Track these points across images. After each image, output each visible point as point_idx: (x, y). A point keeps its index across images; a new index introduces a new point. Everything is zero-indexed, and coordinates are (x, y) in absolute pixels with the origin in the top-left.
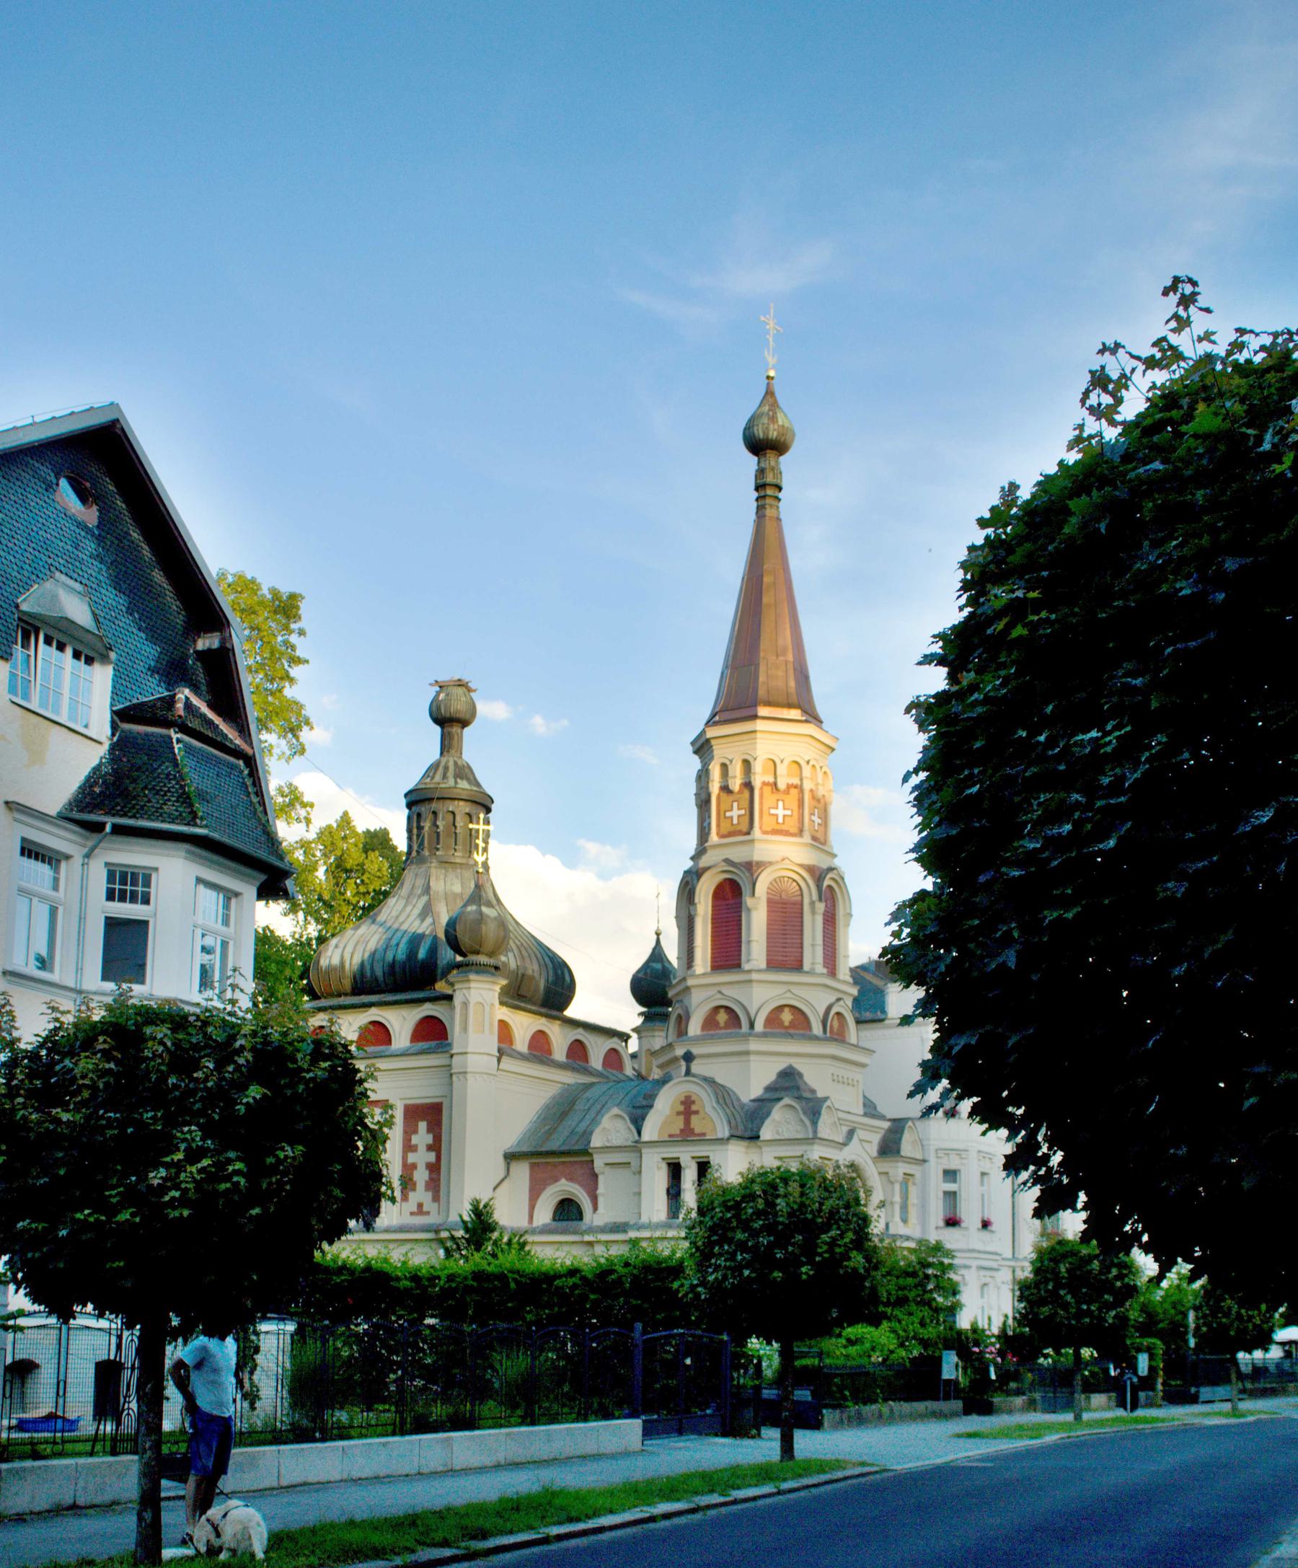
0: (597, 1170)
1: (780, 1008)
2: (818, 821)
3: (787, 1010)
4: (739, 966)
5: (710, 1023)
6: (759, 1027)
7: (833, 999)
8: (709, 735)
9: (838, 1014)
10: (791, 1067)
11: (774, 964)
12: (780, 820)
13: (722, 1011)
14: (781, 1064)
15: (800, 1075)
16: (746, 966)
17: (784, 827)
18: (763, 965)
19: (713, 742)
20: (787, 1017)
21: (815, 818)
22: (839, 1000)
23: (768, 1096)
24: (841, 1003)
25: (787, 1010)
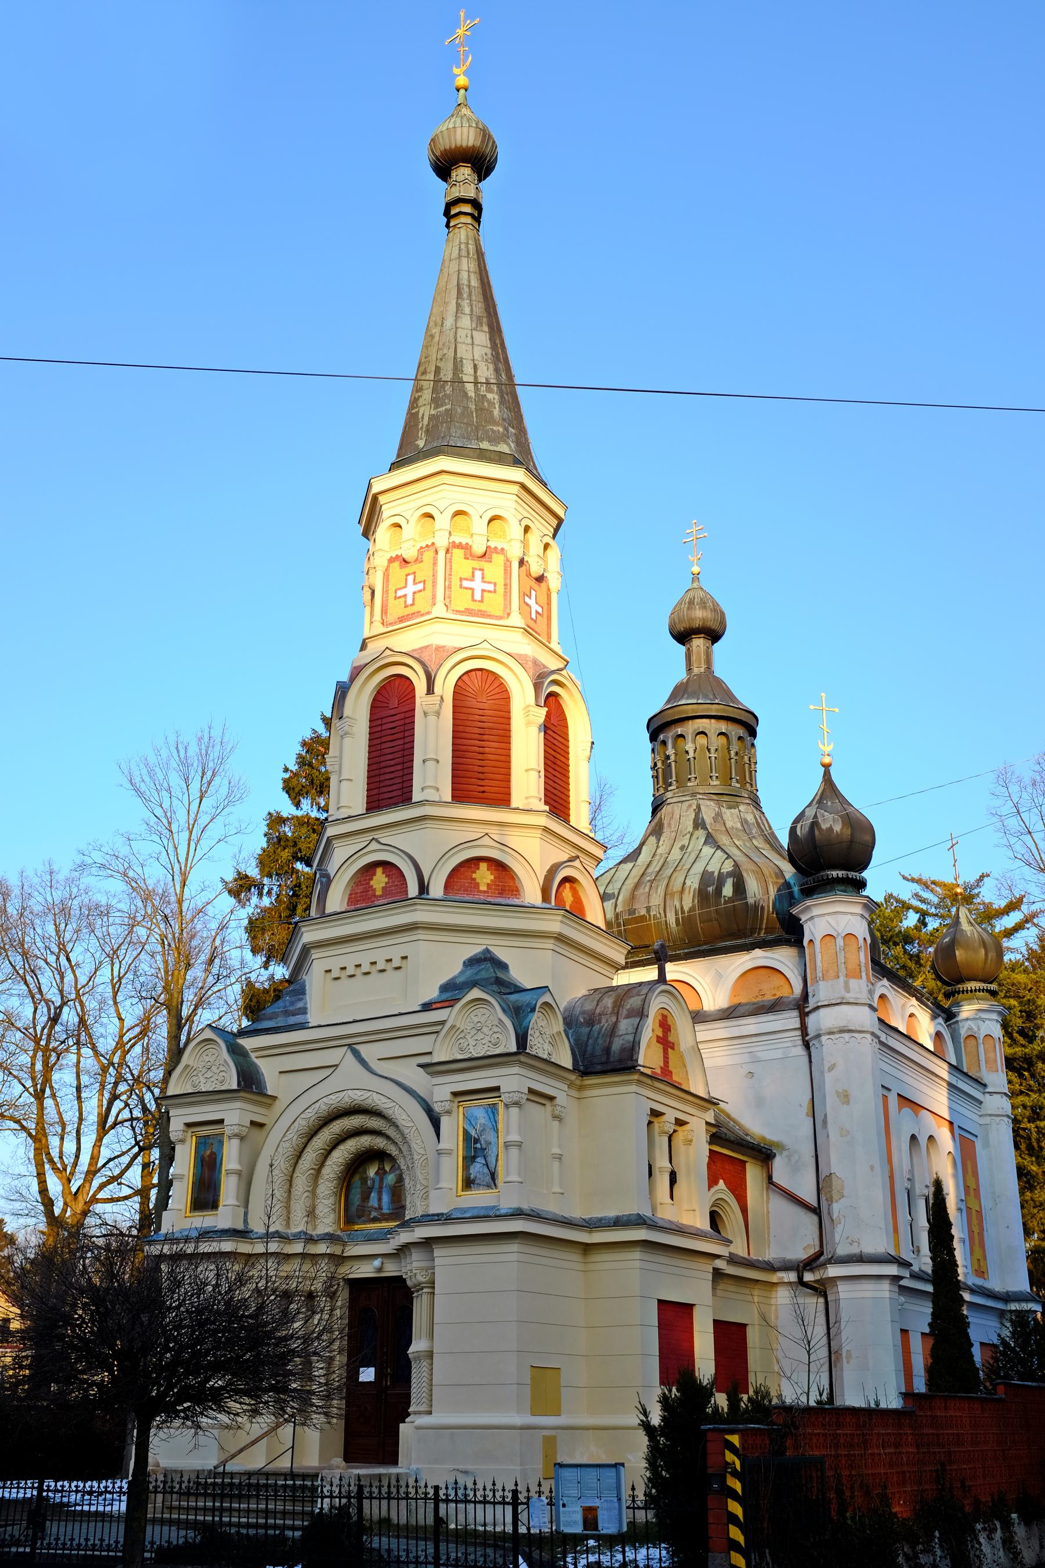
0: (173, 1136)
1: (474, 862)
2: (535, 607)
3: (483, 866)
4: (405, 798)
5: (362, 898)
6: (437, 889)
7: (566, 857)
8: (375, 490)
9: (567, 880)
10: (487, 951)
11: (461, 794)
12: (478, 597)
13: (379, 871)
14: (473, 947)
15: (503, 966)
16: (416, 797)
17: (483, 607)
18: (448, 798)
19: (382, 499)
20: (484, 876)
21: (532, 602)
22: (572, 859)
23: (444, 996)
24: (577, 863)
25: (483, 866)
